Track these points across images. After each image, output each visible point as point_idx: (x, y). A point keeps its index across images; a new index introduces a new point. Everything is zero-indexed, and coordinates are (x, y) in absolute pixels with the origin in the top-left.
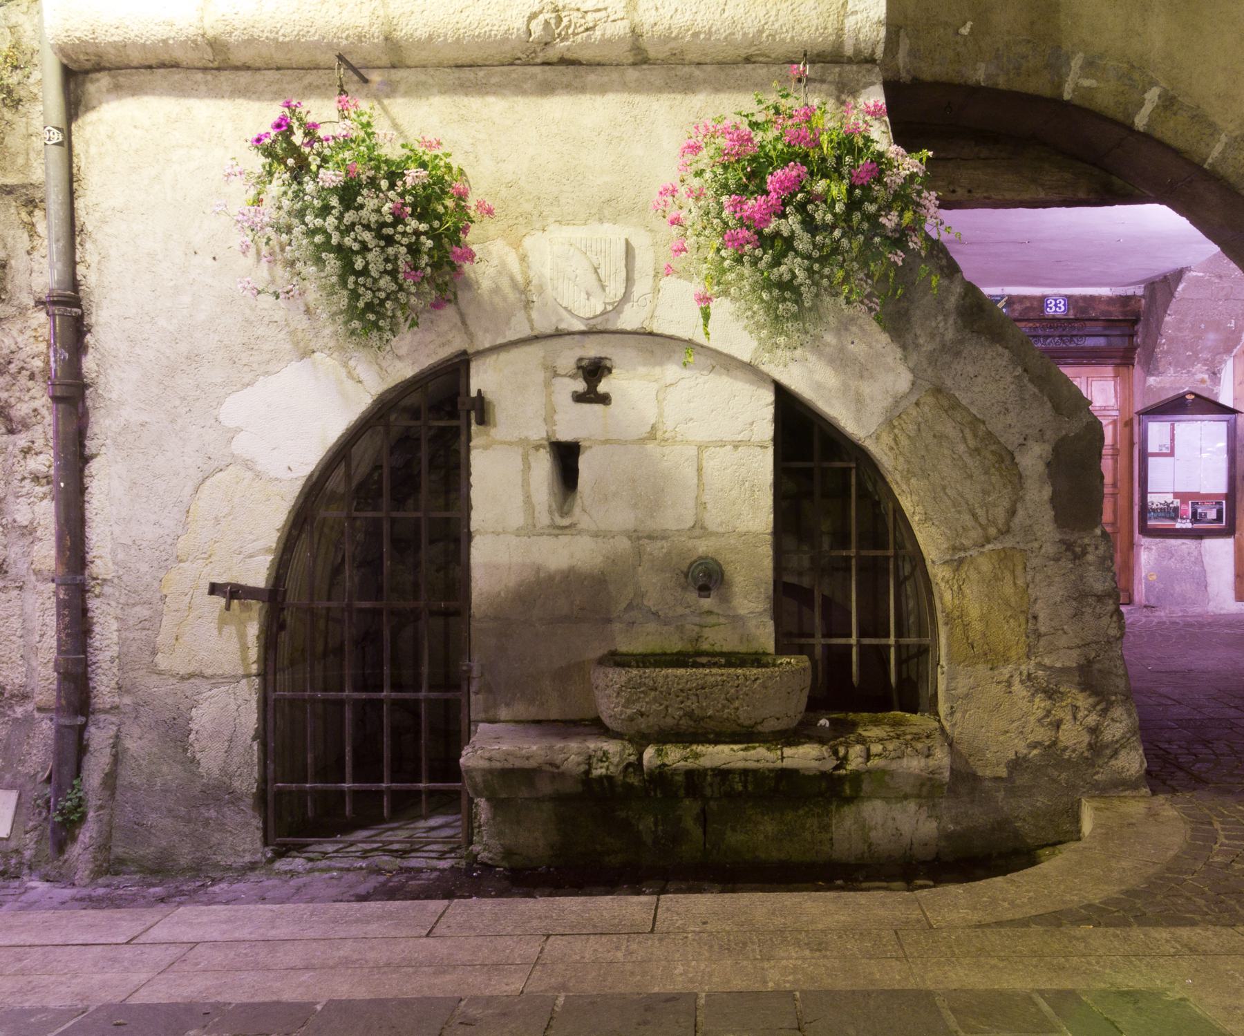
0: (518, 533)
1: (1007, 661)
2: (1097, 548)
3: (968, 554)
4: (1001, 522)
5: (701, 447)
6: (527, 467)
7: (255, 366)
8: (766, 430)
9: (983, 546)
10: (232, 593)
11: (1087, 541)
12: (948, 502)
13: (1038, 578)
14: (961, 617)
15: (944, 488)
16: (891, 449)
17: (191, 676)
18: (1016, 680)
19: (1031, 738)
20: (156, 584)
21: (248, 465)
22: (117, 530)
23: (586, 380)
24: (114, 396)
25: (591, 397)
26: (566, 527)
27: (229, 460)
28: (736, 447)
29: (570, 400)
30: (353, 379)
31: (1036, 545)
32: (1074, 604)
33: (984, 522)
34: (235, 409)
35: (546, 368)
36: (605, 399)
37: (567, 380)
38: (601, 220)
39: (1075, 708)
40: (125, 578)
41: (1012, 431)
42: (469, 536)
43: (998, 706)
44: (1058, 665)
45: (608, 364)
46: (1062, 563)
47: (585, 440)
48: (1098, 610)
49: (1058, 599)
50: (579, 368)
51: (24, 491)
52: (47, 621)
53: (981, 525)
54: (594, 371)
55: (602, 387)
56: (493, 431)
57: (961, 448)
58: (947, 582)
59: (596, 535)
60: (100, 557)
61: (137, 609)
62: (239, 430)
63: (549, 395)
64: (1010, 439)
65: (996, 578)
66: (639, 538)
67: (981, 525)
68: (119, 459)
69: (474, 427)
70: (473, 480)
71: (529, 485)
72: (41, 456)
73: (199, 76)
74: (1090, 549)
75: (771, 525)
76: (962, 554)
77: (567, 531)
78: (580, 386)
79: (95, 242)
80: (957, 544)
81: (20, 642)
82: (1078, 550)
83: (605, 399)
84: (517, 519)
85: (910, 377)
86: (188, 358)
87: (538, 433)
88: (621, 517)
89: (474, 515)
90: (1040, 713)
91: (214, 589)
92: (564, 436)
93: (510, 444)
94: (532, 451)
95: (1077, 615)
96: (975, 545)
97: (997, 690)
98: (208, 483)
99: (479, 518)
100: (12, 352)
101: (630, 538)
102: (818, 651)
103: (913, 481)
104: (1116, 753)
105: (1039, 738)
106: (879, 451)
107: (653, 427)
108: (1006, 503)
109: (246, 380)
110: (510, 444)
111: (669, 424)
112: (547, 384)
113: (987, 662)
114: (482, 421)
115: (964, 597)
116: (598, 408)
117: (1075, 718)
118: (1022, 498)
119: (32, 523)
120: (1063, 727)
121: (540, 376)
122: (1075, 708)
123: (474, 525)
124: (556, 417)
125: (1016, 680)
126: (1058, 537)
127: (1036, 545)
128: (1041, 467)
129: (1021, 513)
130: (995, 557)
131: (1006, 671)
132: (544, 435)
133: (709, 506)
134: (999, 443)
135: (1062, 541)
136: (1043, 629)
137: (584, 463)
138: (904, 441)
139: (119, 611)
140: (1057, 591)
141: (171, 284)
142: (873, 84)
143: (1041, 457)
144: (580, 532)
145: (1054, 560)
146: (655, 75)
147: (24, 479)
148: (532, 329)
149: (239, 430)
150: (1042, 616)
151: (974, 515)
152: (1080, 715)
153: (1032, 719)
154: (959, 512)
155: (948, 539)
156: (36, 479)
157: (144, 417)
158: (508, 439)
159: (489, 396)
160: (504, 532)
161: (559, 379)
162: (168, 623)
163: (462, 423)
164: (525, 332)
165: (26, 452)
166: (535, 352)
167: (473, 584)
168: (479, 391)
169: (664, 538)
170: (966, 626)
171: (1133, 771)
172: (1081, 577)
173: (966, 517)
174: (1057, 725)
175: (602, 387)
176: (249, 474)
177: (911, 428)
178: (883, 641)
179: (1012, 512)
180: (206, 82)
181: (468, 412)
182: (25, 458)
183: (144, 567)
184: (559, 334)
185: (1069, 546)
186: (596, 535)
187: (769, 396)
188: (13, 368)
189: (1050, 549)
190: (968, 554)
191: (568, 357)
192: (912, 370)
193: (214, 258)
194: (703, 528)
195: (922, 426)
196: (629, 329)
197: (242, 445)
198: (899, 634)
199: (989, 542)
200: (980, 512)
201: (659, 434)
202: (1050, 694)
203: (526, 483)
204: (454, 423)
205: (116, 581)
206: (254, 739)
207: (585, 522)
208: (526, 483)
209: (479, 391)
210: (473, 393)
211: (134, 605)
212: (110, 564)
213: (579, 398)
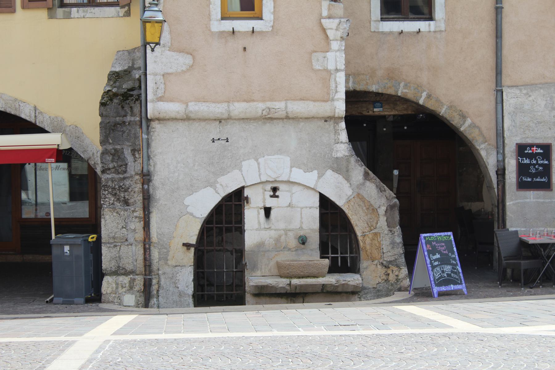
0: (257, 230)
1: (376, 259)
2: (397, 232)
3: (367, 234)
4: (374, 225)
5: (302, 208)
6: (259, 214)
7: (193, 190)
8: (318, 204)
9: (370, 232)
10: (187, 246)
11: (395, 230)
12: (362, 221)
13: (384, 239)
14: (365, 249)
15: (360, 218)
16: (348, 208)
17: (176, 266)
18: (378, 264)
19: (382, 278)
20: (168, 244)
21: (191, 214)
22: (158, 230)
23: (273, 192)
24: (158, 197)
25: (274, 196)
26: (268, 228)
27: (186, 213)
28: (310, 208)
29: (269, 197)
30: (217, 193)
31: (383, 231)
32: (392, 245)
33: (370, 226)
34: (188, 201)
35: (263, 189)
36: (277, 197)
37: (268, 192)
38: (277, 154)
39: (393, 271)
40: (160, 242)
41: (377, 204)
42: (244, 231)
43: (374, 271)
44: (388, 260)
45: (278, 188)
46: (389, 235)
47: (273, 207)
48: (398, 247)
49: (388, 244)
50: (271, 189)
51: (133, 221)
52: (139, 253)
53: (370, 227)
54: (275, 190)
55: (277, 194)
56: (250, 205)
57: (365, 208)
58: (361, 241)
59: (275, 230)
60: (154, 237)
61: (163, 250)
62: (189, 206)
63: (264, 196)
64: (376, 206)
65: (373, 239)
66: (286, 231)
67: (370, 227)
68: (159, 213)
69: (245, 204)
70: (245, 217)
71: (259, 218)
72: (137, 212)
73: (180, 121)
74: (396, 232)
75: (319, 227)
76: (365, 234)
77: (268, 229)
78: (272, 193)
79: (153, 160)
80: (364, 231)
81: (131, 258)
82: (393, 232)
83: (277, 197)
84: (256, 226)
85: (352, 191)
86: (177, 188)
87: (262, 205)
88: (282, 225)
89: (246, 225)
90: (384, 272)
91: (184, 245)
92: (268, 206)
93: (254, 208)
94: (260, 210)
95: (393, 248)
96: (368, 231)
97: (373, 267)
98: (181, 218)
99: (246, 227)
100: (129, 186)
101: (284, 231)
102: (330, 258)
103: (353, 216)
104: (402, 281)
105: (384, 278)
106: (345, 209)
107: (290, 203)
108: (375, 221)
109: (191, 193)
110: (254, 208)
111: (293, 203)
112: (264, 193)
113: (371, 260)
114: (247, 203)
115: (366, 244)
116: (277, 198)
117: (393, 273)
118: (379, 220)
119: (135, 229)
120: (390, 275)
121: (261, 191)
122: (393, 271)
123: (246, 228)
124: (266, 201)
125: (378, 264)
126: (388, 229)
127: (383, 231)
128: (384, 213)
129: (379, 224)
130: (373, 234)
131: (376, 262)
132: (263, 206)
133: (303, 223)
134: (373, 207)
135: (389, 230)
136: (384, 252)
137: (273, 213)
138: (351, 207)
139: (158, 251)
140: (388, 242)
141: (173, 171)
142: (342, 122)
143: (384, 210)
144: (272, 229)
145: (387, 235)
146: (291, 121)
147: (133, 217)
148: (261, 180)
149: (189, 206)
150: (384, 248)
151: (368, 224)
152: (394, 272)
153: (382, 273)
154: (364, 224)
155: (362, 230)
156: (136, 217)
157: (166, 203)
158: (254, 207)
159: (249, 196)
160: (253, 229)
161: (266, 192)
162: (171, 253)
163: (242, 203)
164: (259, 181)
165: (133, 211)
166: (261, 185)
167: (245, 243)
168: (247, 195)
169: (292, 231)
170: (366, 251)
171: (406, 286)
172: (394, 239)
173: (366, 225)
174: (388, 275)
175: (277, 194)
176: (192, 216)
177: (352, 203)
178: (346, 255)
179: (377, 223)
180: (182, 122)
181: (244, 200)
182: (133, 213)
183: (165, 239)
184: (267, 181)
185: (391, 231)
186: (275, 230)
187: (318, 196)
188: (130, 190)
189: (386, 232)
190: (367, 234)
191: (269, 187)
192: (353, 190)
193: (184, 164)
194: (302, 228)
195: (355, 203)
196: (284, 180)
197: (190, 209)
198: (351, 253)
199: (371, 231)
200: (369, 223)
201: (291, 205)
202: (387, 267)
203: (258, 217)
204: (241, 203)
205: (158, 243)
206: (192, 281)
207: (273, 227)
208: (258, 217)
209: (247, 195)
210: (245, 196)
211: (162, 249)
212: (156, 239)
213: (271, 196)
